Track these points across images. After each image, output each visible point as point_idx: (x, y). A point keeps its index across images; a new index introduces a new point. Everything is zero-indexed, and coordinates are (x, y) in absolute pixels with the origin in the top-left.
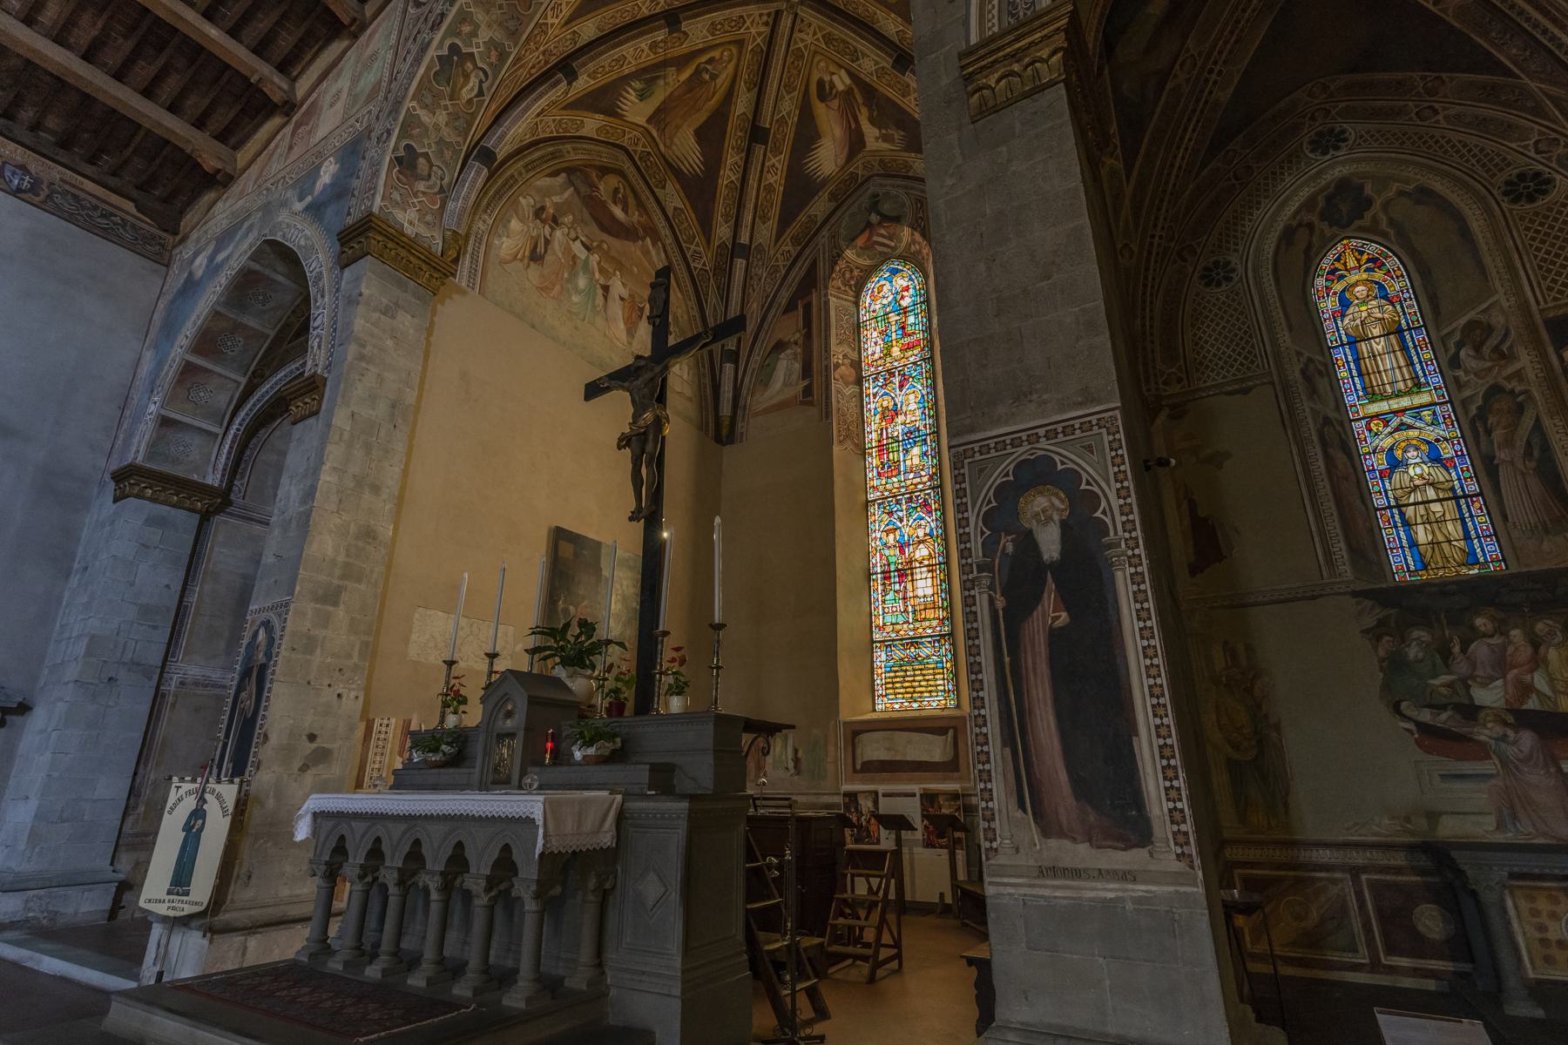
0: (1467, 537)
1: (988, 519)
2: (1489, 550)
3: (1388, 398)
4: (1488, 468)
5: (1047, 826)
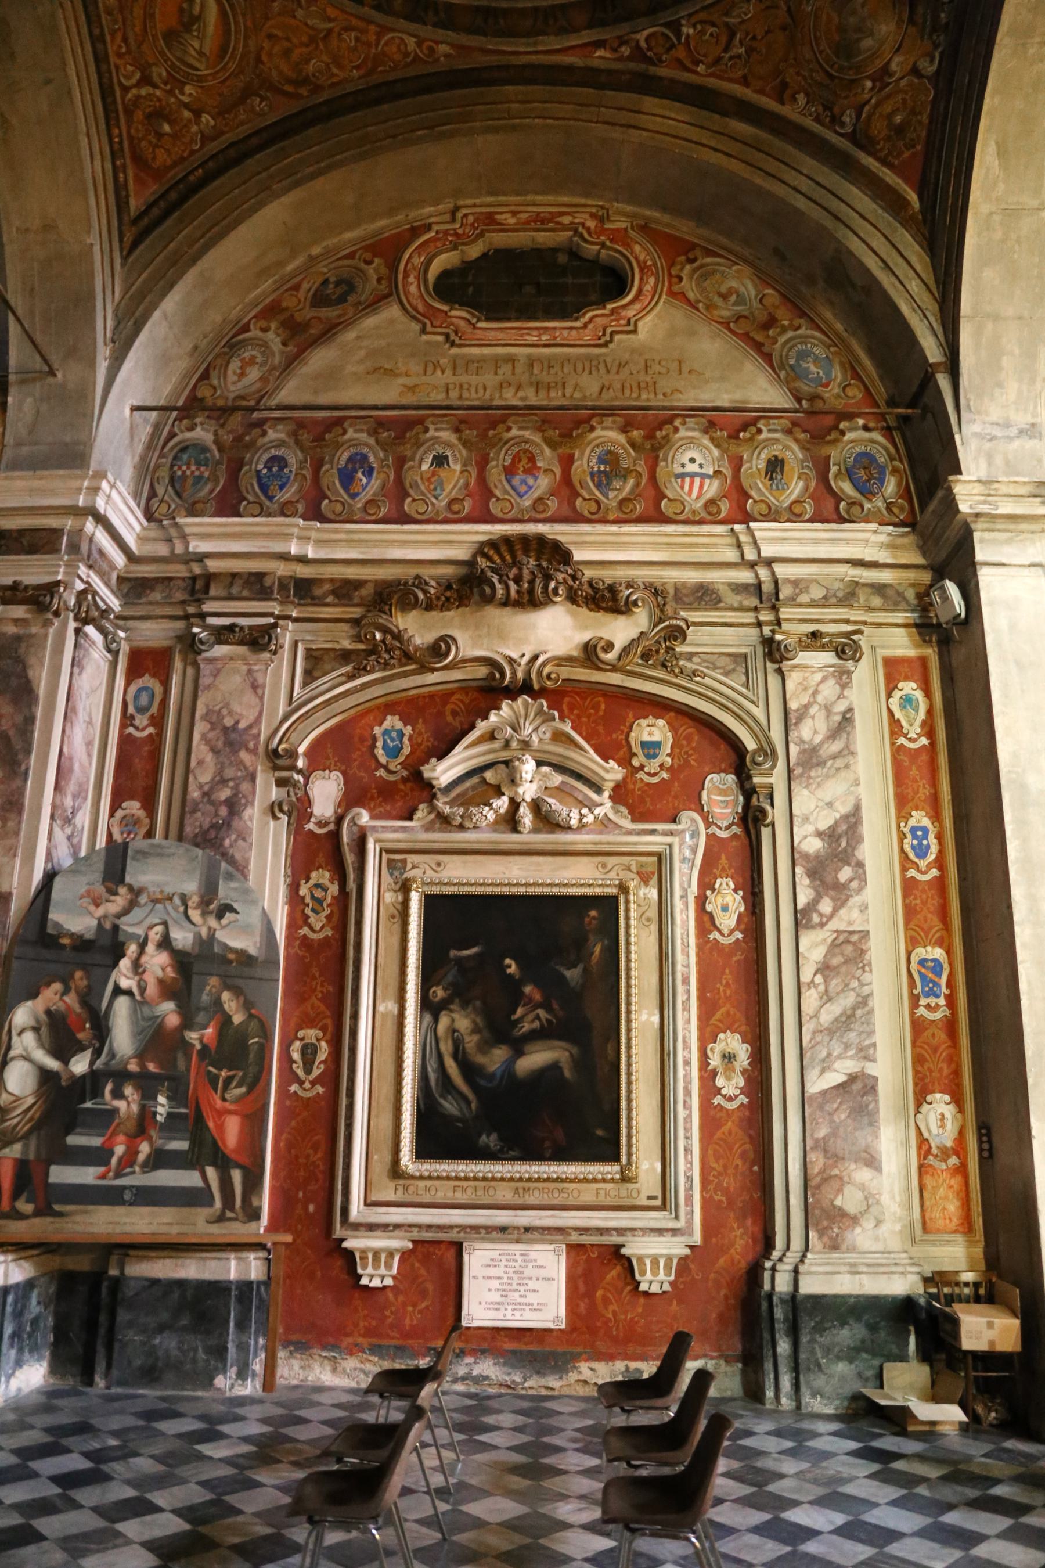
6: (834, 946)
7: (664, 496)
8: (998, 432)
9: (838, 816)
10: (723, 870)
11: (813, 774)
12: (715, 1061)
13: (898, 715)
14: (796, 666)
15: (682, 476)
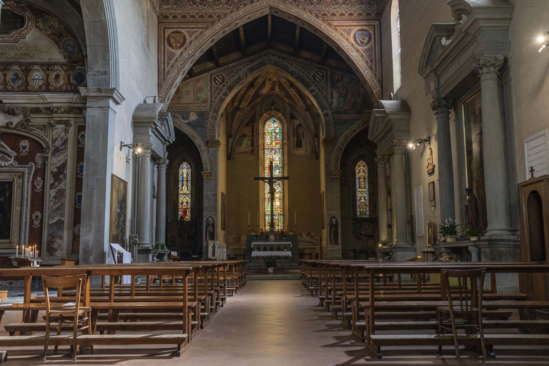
0: (366, 211)
1: (329, 220)
2: (368, 213)
3: (361, 189)
4: (370, 202)
5: (332, 244)
6: (57, 193)
7: (29, 85)
9: (61, 163)
10: (39, 175)
11: (57, 154)
13: (80, 139)
14: (55, 128)
15: (34, 79)
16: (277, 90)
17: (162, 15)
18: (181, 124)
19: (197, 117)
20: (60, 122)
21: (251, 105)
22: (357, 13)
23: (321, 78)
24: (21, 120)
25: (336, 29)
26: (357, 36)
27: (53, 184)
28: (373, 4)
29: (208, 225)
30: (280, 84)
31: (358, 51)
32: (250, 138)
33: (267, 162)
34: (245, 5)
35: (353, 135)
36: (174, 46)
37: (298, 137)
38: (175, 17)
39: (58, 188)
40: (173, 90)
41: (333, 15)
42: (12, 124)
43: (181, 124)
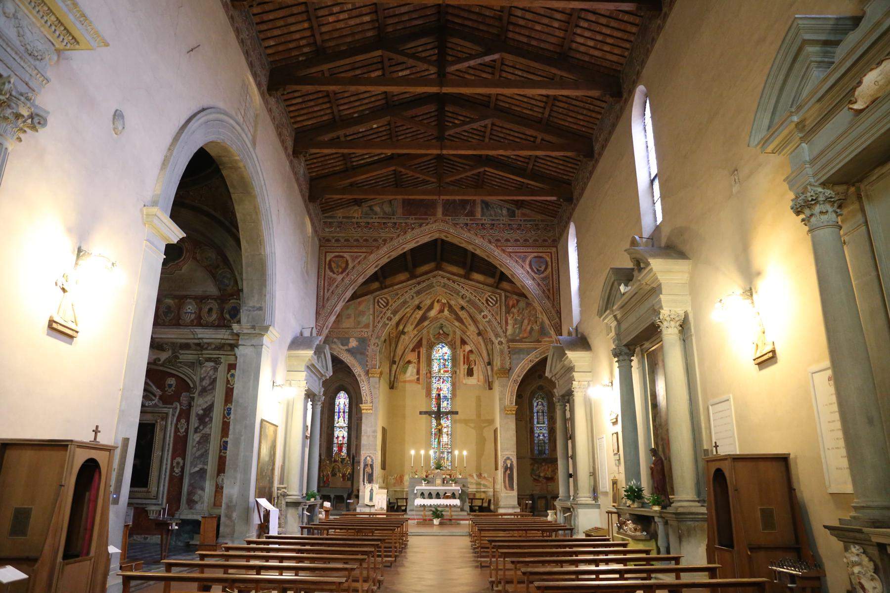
6: (202, 437)
8: (251, 309)
12: (175, 464)
13: (229, 379)
15: (186, 313)
16: (446, 312)
17: (324, 238)
18: (340, 350)
19: (357, 343)
20: (209, 360)
21: (419, 327)
22: (533, 239)
23: (494, 303)
24: (169, 357)
25: (511, 256)
26: (533, 264)
27: (198, 428)
28: (550, 231)
29: (366, 465)
30: (450, 306)
31: (534, 279)
32: (416, 366)
33: (434, 392)
34: (413, 229)
35: (530, 366)
36: (335, 271)
37: (469, 365)
38: (337, 240)
39: (203, 432)
40: (333, 318)
41: (507, 240)
42: (159, 360)
43: (340, 350)
